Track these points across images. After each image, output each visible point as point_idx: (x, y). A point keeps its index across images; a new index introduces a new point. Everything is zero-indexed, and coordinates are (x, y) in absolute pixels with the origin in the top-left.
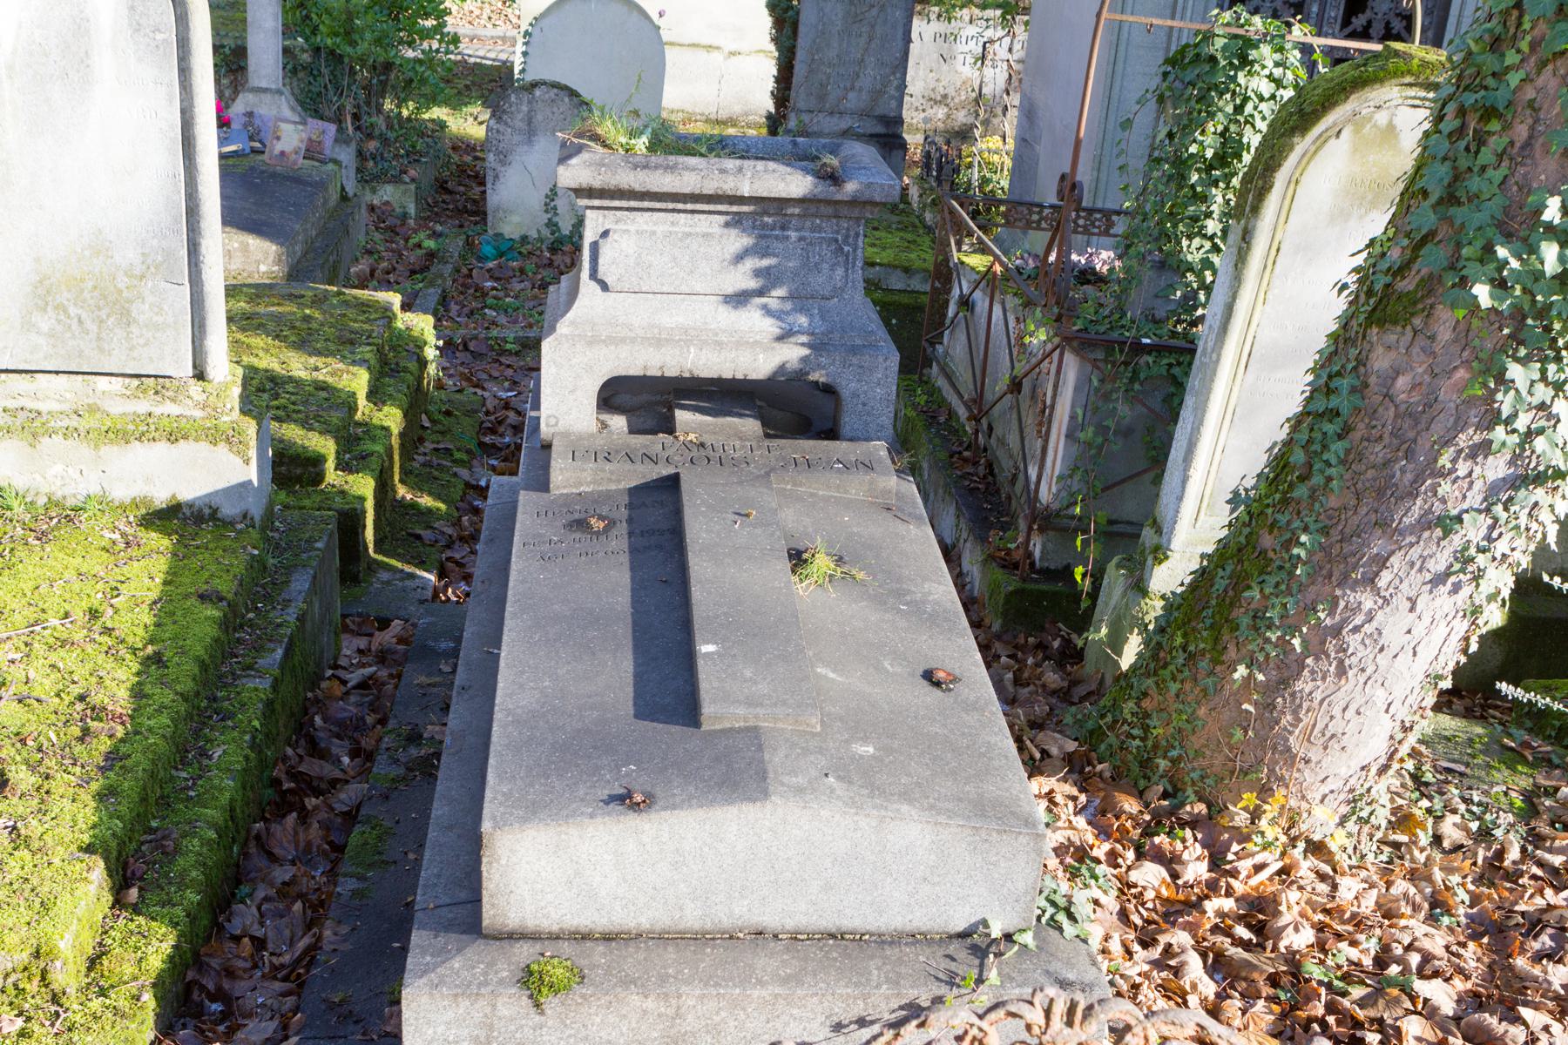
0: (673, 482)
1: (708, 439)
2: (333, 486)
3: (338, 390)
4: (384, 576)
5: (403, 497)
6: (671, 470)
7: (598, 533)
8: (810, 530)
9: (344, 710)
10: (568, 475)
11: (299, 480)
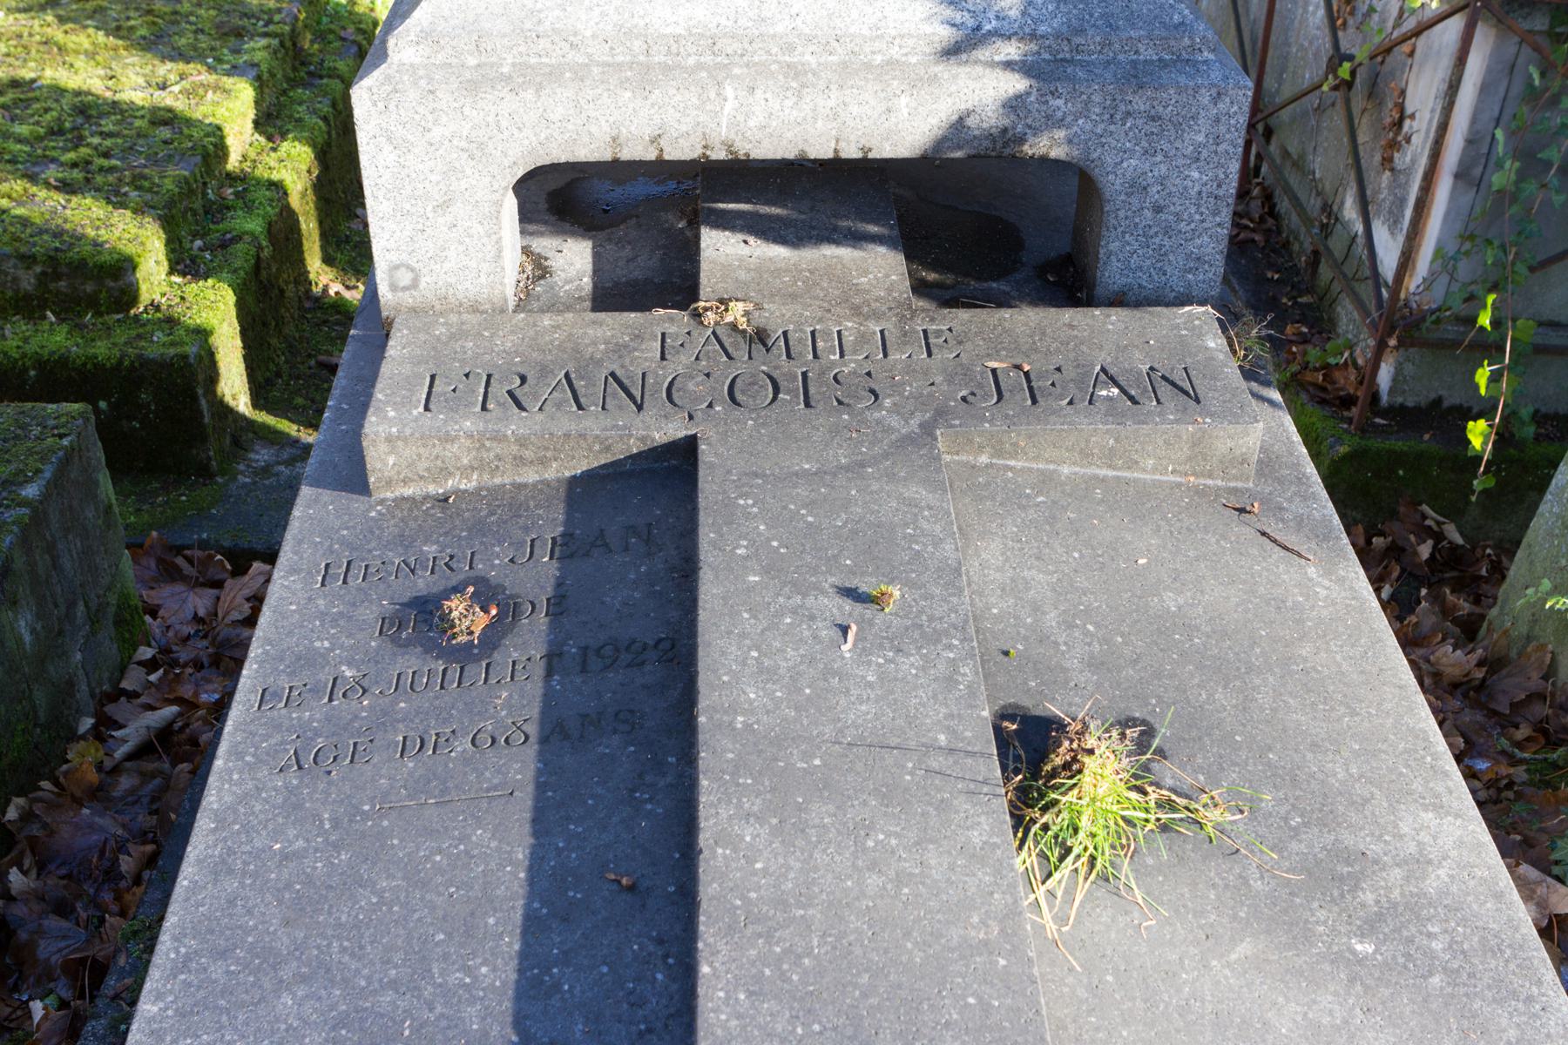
0: (686, 450)
1: (776, 316)
2: (157, 308)
3: (189, 122)
4: (262, 455)
5: (326, 289)
6: (672, 430)
7: (464, 655)
8: (1051, 618)
9: (91, 826)
10: (409, 452)
11: (93, 303)
